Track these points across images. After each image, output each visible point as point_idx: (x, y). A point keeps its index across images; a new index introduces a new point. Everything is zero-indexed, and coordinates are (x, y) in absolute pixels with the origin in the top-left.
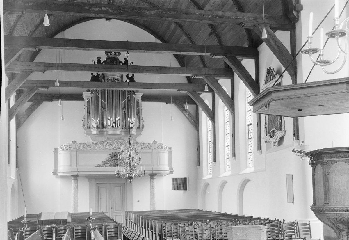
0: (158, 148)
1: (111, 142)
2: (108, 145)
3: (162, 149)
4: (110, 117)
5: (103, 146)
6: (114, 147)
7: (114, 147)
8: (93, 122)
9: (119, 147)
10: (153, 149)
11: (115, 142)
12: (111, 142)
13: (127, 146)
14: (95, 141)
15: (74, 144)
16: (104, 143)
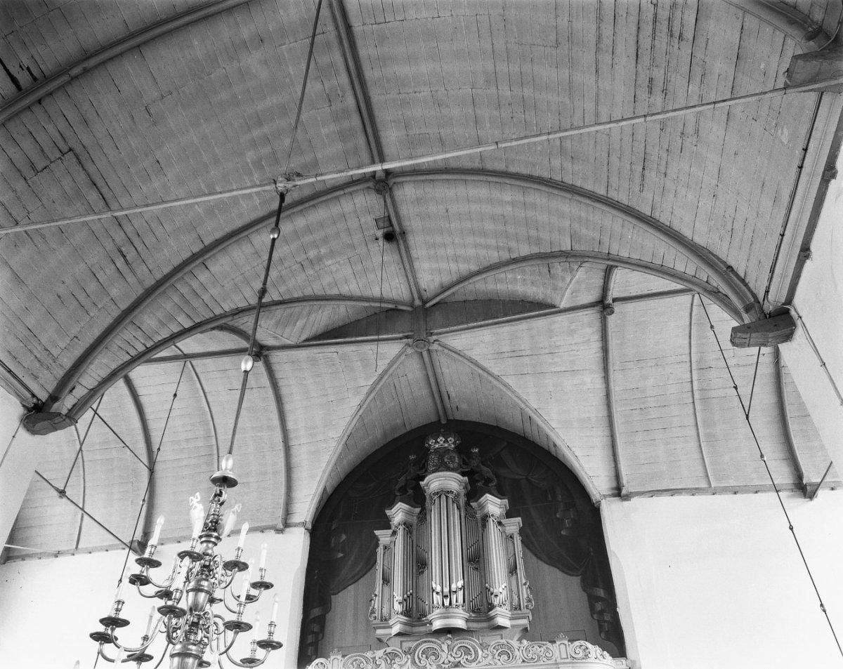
0: (572, 657)
1: (435, 646)
2: (427, 658)
3: (589, 660)
4: (436, 583)
5: (414, 662)
6: (443, 663)
7: (441, 662)
8: (395, 600)
9: (457, 660)
10: (559, 660)
11: (445, 647)
12: (435, 646)
13: (480, 657)
14: (392, 648)
15: (336, 660)
16: (415, 650)
